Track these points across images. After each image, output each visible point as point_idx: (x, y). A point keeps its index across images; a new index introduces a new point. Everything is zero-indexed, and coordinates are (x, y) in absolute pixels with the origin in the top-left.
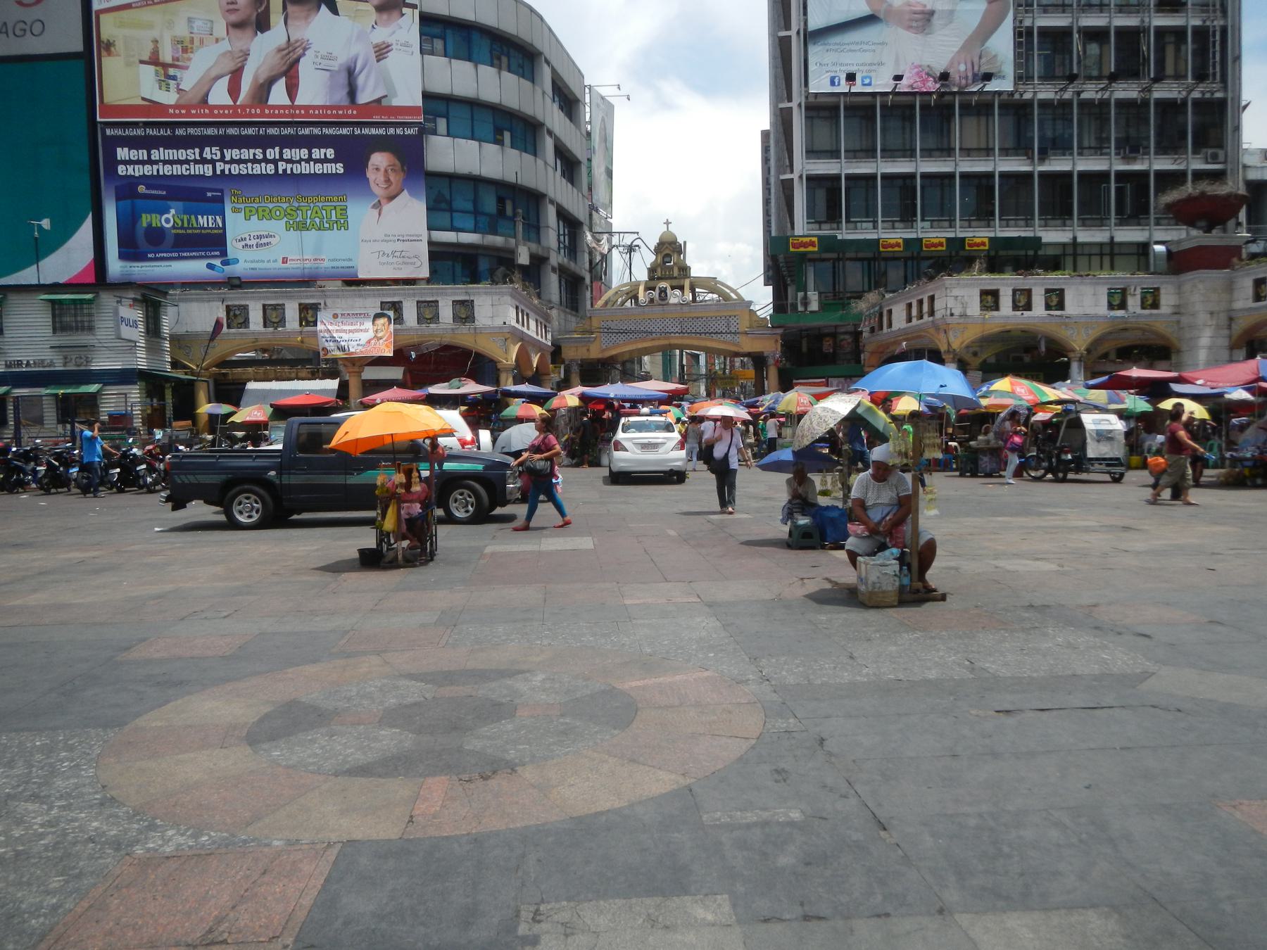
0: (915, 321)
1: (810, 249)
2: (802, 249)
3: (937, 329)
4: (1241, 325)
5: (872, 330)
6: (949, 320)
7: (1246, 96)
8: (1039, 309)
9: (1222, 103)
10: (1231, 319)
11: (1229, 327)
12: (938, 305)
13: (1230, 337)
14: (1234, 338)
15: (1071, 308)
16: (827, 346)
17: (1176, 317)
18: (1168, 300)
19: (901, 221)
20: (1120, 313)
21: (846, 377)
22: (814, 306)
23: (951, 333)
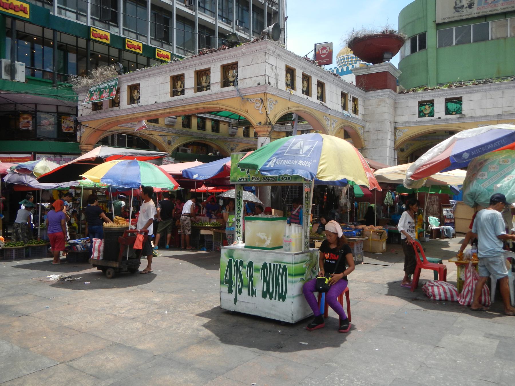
0: (190, 93)
1: (21, 14)
2: (11, 12)
3: (244, 99)
4: (402, 136)
5: (97, 107)
6: (269, 90)
7: (289, 13)
8: (314, 98)
9: (276, 13)
10: (396, 129)
11: (395, 134)
12: (242, 72)
13: (395, 140)
14: (398, 143)
15: (328, 103)
16: (25, 123)
17: (363, 123)
18: (360, 109)
19: (100, 21)
20: (345, 112)
21: (55, 154)
22: (21, 76)
23: (268, 104)
